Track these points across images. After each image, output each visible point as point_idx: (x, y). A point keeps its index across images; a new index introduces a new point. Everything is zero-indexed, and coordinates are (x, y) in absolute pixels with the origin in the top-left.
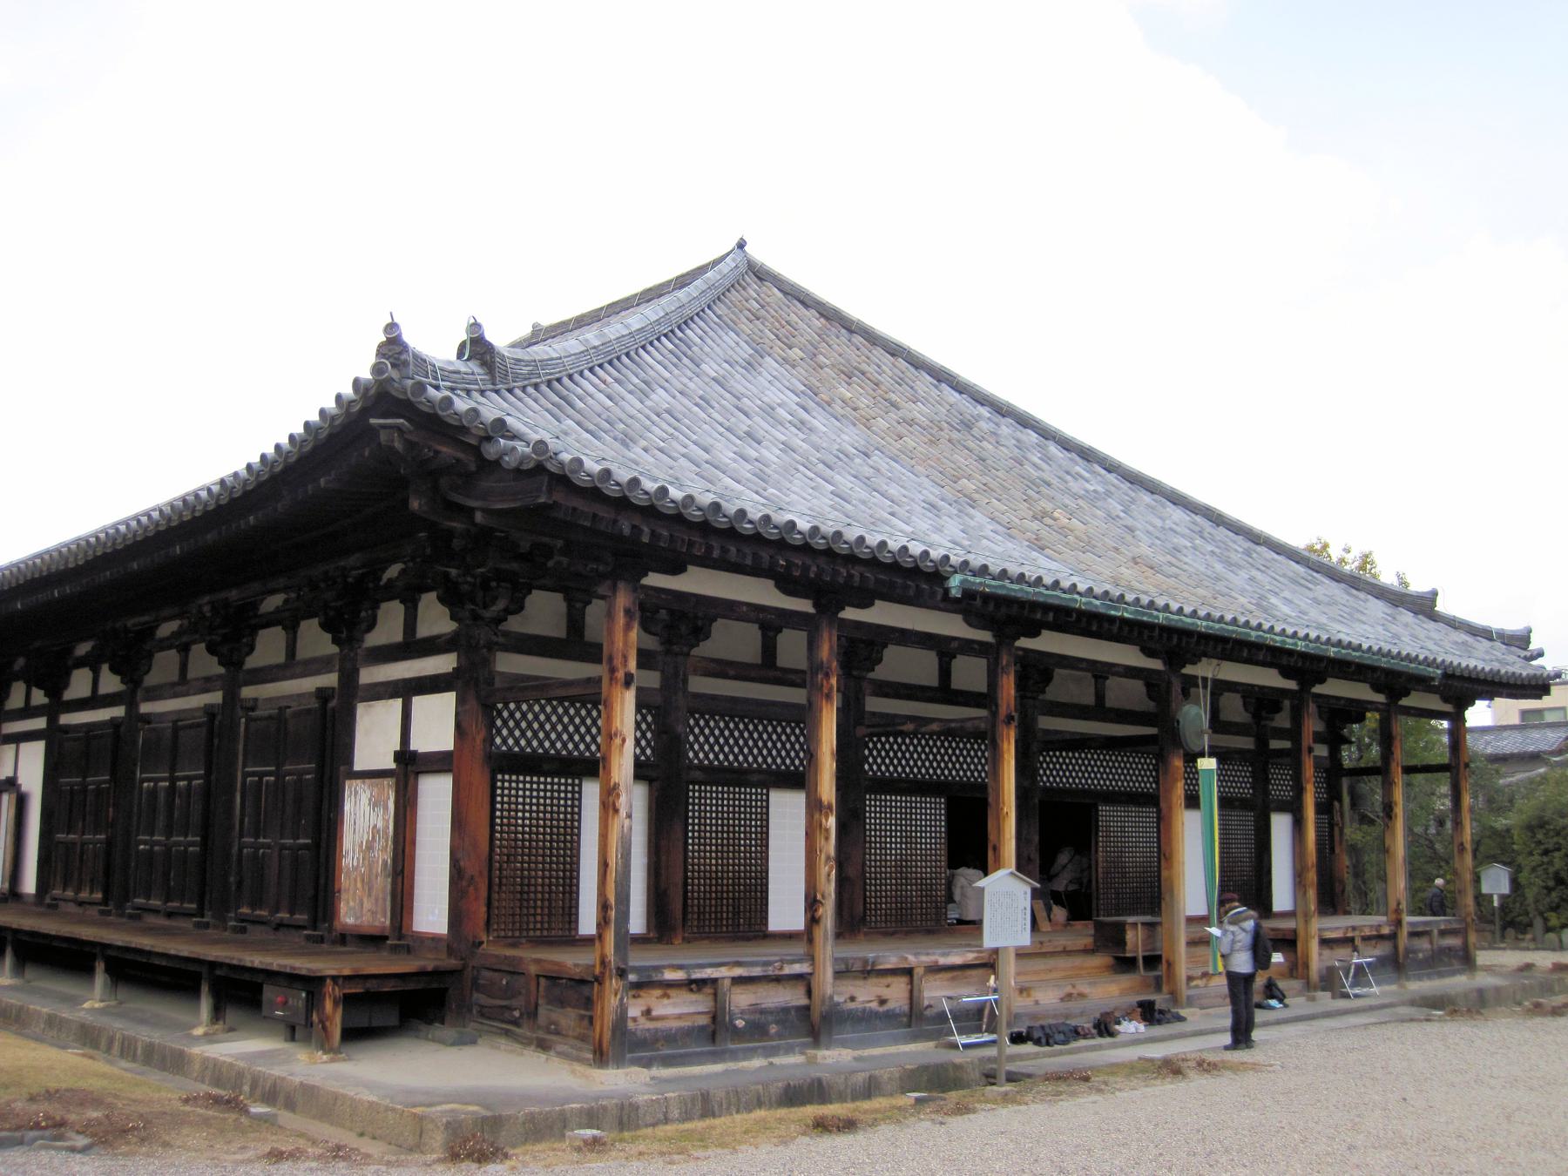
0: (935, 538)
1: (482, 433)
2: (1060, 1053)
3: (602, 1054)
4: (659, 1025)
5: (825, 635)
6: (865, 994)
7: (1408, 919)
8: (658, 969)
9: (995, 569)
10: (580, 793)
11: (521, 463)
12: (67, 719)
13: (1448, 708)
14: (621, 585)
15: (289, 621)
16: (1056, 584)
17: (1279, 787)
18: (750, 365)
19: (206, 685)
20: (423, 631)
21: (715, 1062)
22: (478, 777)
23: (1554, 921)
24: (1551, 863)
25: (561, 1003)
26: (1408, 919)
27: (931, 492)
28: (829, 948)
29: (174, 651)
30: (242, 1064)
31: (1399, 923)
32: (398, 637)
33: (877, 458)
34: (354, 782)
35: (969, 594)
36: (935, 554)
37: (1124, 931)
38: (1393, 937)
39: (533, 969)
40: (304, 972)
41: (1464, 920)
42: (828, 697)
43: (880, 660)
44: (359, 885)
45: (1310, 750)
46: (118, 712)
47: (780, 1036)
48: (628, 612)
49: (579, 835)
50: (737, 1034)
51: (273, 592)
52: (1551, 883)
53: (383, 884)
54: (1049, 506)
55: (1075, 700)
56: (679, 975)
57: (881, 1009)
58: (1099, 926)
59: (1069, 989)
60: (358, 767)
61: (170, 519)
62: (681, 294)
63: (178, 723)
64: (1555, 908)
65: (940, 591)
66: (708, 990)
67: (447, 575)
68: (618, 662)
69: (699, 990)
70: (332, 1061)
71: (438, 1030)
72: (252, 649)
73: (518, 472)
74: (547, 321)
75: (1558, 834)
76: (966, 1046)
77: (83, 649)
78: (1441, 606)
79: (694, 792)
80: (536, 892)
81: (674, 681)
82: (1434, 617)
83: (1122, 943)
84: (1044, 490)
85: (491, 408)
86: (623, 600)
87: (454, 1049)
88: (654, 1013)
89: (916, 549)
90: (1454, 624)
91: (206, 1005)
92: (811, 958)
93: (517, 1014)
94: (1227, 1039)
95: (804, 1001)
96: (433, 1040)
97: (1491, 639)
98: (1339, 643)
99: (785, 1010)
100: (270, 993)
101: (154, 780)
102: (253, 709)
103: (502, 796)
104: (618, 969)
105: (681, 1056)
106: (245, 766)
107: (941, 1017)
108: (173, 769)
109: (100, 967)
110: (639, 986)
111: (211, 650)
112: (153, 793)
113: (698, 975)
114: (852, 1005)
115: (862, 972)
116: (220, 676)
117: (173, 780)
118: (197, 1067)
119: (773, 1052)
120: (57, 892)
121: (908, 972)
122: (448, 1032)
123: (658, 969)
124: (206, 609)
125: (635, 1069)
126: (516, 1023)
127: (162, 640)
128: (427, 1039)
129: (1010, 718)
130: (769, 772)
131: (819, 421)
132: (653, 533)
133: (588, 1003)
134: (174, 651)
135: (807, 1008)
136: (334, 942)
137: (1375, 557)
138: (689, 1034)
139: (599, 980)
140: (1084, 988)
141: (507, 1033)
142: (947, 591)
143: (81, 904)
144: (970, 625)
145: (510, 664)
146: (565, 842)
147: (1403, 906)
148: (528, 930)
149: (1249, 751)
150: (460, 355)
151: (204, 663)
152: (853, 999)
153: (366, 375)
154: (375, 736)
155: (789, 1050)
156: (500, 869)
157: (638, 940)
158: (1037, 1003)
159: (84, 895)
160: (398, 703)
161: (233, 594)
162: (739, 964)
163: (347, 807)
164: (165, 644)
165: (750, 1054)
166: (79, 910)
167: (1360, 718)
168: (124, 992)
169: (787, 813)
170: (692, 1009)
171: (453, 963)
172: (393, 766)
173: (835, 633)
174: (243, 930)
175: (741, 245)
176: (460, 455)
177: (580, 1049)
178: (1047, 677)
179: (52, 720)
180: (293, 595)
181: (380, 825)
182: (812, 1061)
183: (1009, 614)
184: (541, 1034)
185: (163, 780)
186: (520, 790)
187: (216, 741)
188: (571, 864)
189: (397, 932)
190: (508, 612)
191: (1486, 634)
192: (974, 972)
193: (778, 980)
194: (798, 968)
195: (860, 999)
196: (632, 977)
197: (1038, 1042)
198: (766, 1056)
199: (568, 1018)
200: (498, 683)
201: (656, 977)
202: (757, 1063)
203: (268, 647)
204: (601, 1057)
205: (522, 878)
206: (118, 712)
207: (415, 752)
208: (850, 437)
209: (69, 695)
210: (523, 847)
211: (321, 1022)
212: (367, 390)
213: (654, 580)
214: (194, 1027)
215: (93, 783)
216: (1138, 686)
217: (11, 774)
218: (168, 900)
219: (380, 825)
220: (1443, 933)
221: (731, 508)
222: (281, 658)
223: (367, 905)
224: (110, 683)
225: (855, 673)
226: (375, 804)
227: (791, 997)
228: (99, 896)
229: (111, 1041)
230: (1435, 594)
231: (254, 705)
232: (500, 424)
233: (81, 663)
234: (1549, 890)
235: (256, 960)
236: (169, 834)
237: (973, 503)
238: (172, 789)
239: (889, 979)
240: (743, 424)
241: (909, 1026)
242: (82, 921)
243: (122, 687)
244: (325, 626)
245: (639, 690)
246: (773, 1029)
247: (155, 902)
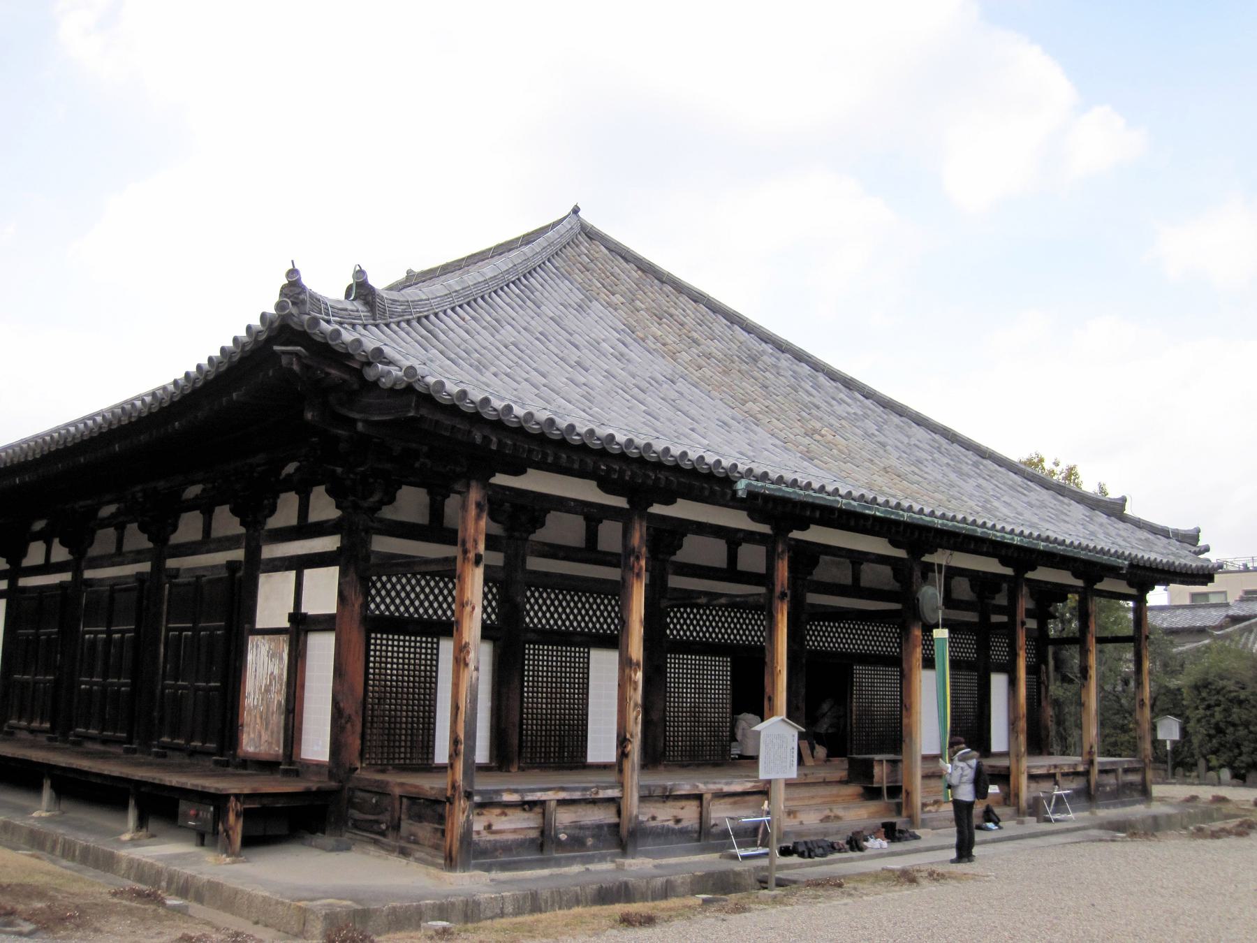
0: (726, 449)
1: (364, 359)
2: (820, 864)
3: (451, 860)
4: (497, 837)
5: (637, 526)
6: (664, 815)
7: (1099, 759)
8: (498, 792)
9: (774, 476)
10: (437, 649)
11: (395, 384)
12: (24, 582)
13: (1133, 591)
14: (473, 483)
15: (206, 508)
16: (822, 488)
17: (998, 652)
18: (580, 308)
19: (138, 556)
20: (314, 517)
21: (542, 868)
22: (356, 636)
23: (1214, 762)
24: (1212, 715)
25: (420, 818)
26: (1099, 759)
27: (726, 413)
28: (636, 777)
29: (112, 529)
30: (160, 864)
31: (1091, 763)
32: (294, 521)
33: (681, 385)
35: (752, 495)
36: (726, 463)
37: (872, 767)
38: (1086, 773)
39: (397, 791)
40: (212, 791)
41: (1143, 761)
42: (638, 575)
43: (680, 546)
44: (258, 720)
45: (1023, 623)
46: (67, 577)
47: (595, 847)
48: (478, 505)
49: (436, 683)
50: (560, 845)
51: (194, 483)
52: (1212, 732)
53: (278, 720)
54: (818, 425)
55: (837, 581)
56: (515, 798)
57: (677, 827)
58: (852, 762)
59: (827, 812)
60: (259, 625)
61: (111, 424)
62: (526, 249)
63: (115, 586)
64: (1215, 752)
65: (729, 492)
66: (538, 810)
67: (334, 471)
68: (469, 545)
69: (531, 810)
70: (234, 862)
71: (320, 839)
72: (175, 529)
73: (392, 391)
74: (418, 269)
75: (1218, 692)
76: (744, 857)
77: (39, 525)
78: (1129, 510)
79: (529, 650)
80: (401, 729)
81: (515, 561)
82: (1123, 518)
83: (870, 776)
84: (814, 412)
85: (371, 339)
86: (475, 495)
87: (333, 855)
88: (494, 828)
89: (710, 459)
90: (1139, 524)
91: (132, 816)
92: (621, 785)
93: (383, 826)
94: (953, 854)
95: (614, 820)
96: (316, 847)
97: (1168, 537)
98: (1047, 539)
99: (600, 827)
100: (183, 806)
101: (92, 633)
102: (176, 577)
103: (375, 651)
104: (466, 792)
105: (515, 862)
106: (168, 622)
107: (725, 834)
108: (109, 626)
109: (47, 784)
110: (482, 806)
111: (143, 528)
112: (93, 643)
113: (529, 797)
114: (653, 824)
115: (662, 797)
116: (149, 550)
117: (109, 633)
118: (124, 866)
119: (589, 860)
120: (13, 722)
121: (699, 797)
122: (328, 840)
123: (498, 792)
124: (140, 494)
125: (478, 873)
126: (383, 834)
127: (103, 519)
128: (310, 845)
129: (783, 595)
130: (590, 634)
131: (635, 353)
132: (500, 442)
133: (441, 819)
134: (112, 529)
135: (617, 825)
136: (236, 767)
137: (1079, 470)
138: (522, 845)
139: (450, 800)
140: (839, 812)
141: (376, 842)
142: (735, 492)
143: (32, 731)
144: (753, 519)
145: (383, 544)
146: (425, 688)
147: (1095, 749)
148: (394, 759)
149: (975, 623)
150: (348, 295)
151: (136, 539)
152: (654, 818)
153: (271, 310)
154: (274, 600)
155: (602, 859)
156: (373, 710)
157: (483, 768)
158: (801, 823)
159: (35, 724)
160: (292, 575)
161: (161, 484)
162: (563, 789)
163: (250, 657)
164: (105, 523)
165: (570, 861)
166: (30, 737)
167: (1064, 599)
168: (65, 805)
169: (603, 667)
170: (525, 825)
171: (333, 784)
172: (287, 625)
173: (645, 524)
174: (164, 756)
175: (576, 211)
176: (346, 377)
177: (433, 856)
178: (814, 562)
179: (12, 584)
180: (210, 486)
181: (276, 672)
182: (620, 868)
183: (783, 511)
184: (403, 844)
185: (101, 632)
186: (390, 646)
187: (145, 602)
188: (430, 706)
189: (288, 760)
190: (382, 503)
191: (1164, 533)
193: (594, 802)
194: (610, 793)
195: (660, 817)
196: (477, 799)
197: (802, 855)
198: (584, 863)
199: (424, 831)
200: (373, 560)
201: (496, 799)
202: (576, 868)
203: (189, 527)
204: (451, 863)
205: (390, 717)
206: (67, 577)
207: (305, 614)
208: (661, 367)
209: (27, 562)
210: (391, 693)
211: (226, 831)
212: (272, 323)
213: (500, 479)
214: (122, 833)
215: (45, 634)
216: (887, 570)
218: (103, 730)
219: (276, 672)
220: (1126, 771)
221: (562, 423)
222: (198, 536)
223: (265, 737)
224: (60, 553)
225: (661, 556)
226: (272, 655)
227: (605, 816)
228: (47, 725)
229: (55, 843)
230: (1124, 500)
231: (176, 573)
232: (379, 351)
233: (37, 537)
234: (1210, 737)
235: (173, 780)
236: (105, 675)
237: (757, 422)
238: (109, 640)
239: (683, 803)
240: (574, 355)
241: (699, 840)
242: (33, 746)
243: (70, 557)
244: (234, 511)
245: (487, 568)
246: (590, 842)
247: (93, 732)
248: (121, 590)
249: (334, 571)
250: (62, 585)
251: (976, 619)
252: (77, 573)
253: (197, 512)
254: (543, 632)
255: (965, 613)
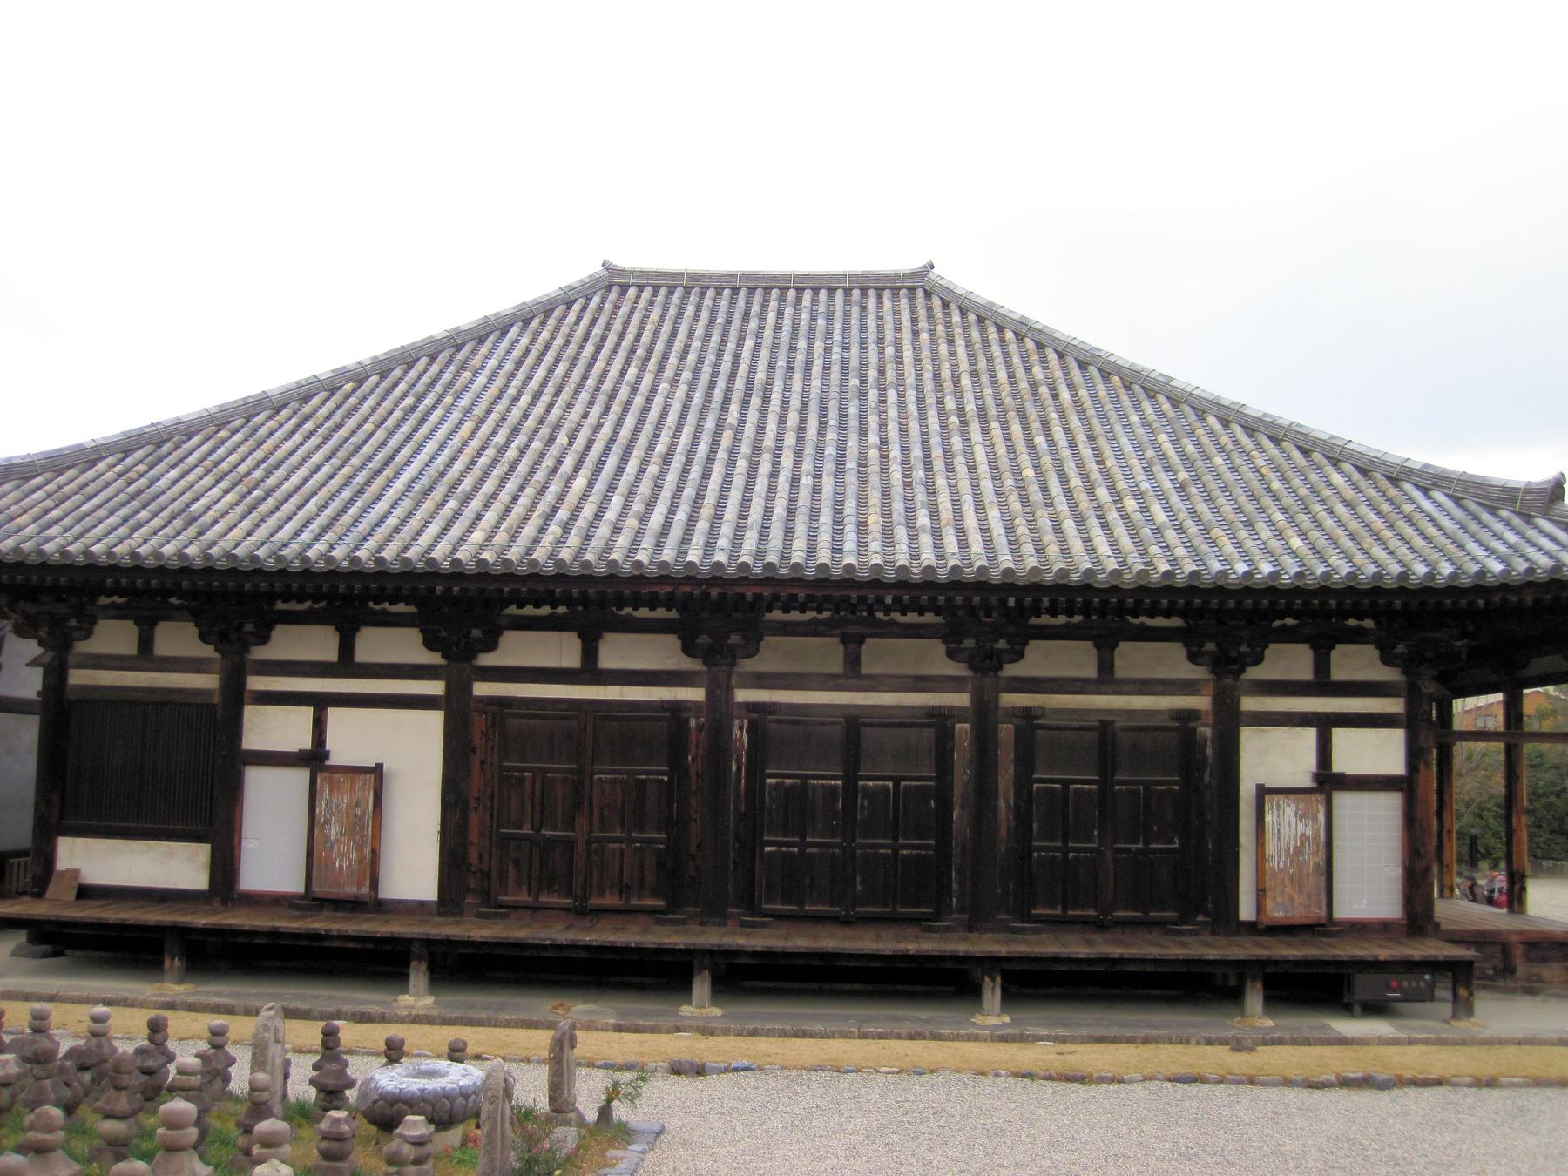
20: (1338, 674)
25: (1544, 960)
34: (1276, 797)
44: (1288, 883)
53: (1315, 883)
102: (1038, 718)
117: (851, 778)
126: (1490, 978)
154: (1273, 757)
160: (1310, 735)
172: (1307, 782)
181: (1309, 832)
217: (306, 744)
226: (1301, 816)
248: (871, 725)
249: (1397, 736)
250: (675, 708)
252: (719, 692)
253: (1090, 644)
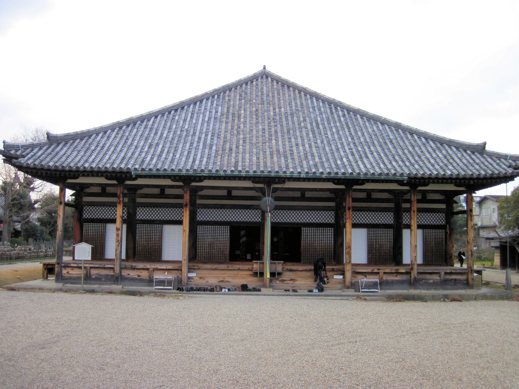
6: (133, 274)
47: (105, 281)
56: (75, 265)
78: (488, 148)
79: (138, 226)
81: (133, 201)
92: (114, 265)
99: (107, 275)
114: (129, 276)
119: (102, 284)
121: (148, 269)
158: (207, 282)
169: (111, 230)
175: (264, 68)
192: (173, 271)
230: (485, 144)
239: (141, 271)
251: (393, 206)
254: (141, 220)
255: (363, 203)
